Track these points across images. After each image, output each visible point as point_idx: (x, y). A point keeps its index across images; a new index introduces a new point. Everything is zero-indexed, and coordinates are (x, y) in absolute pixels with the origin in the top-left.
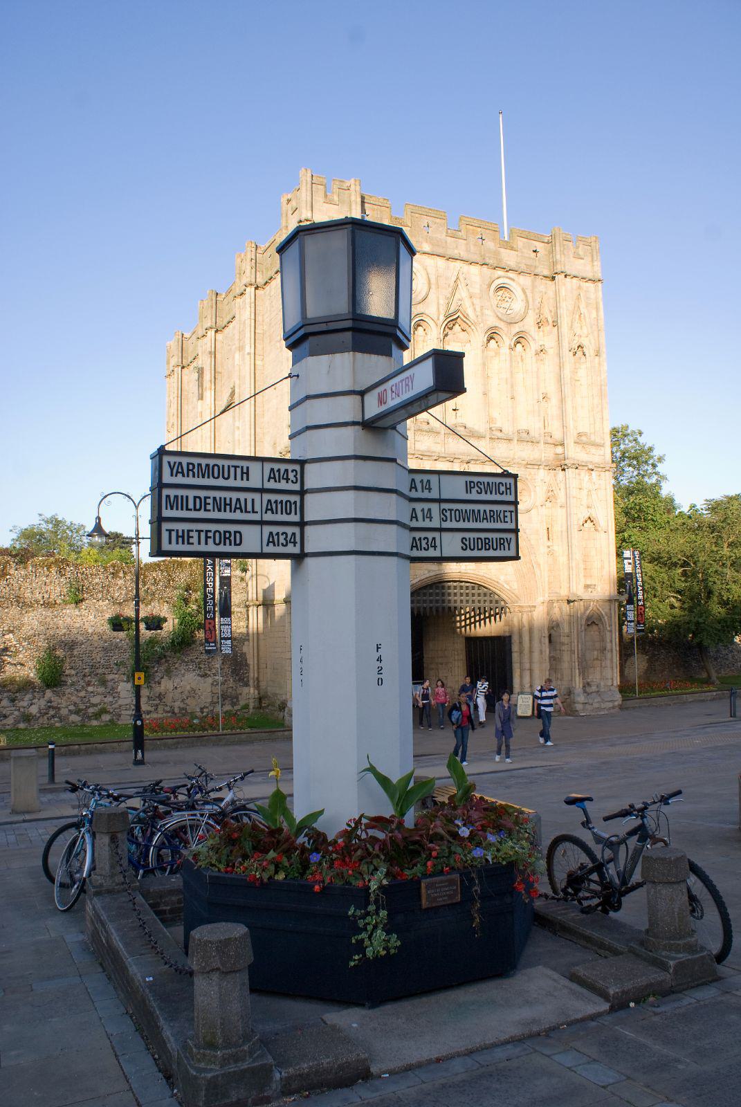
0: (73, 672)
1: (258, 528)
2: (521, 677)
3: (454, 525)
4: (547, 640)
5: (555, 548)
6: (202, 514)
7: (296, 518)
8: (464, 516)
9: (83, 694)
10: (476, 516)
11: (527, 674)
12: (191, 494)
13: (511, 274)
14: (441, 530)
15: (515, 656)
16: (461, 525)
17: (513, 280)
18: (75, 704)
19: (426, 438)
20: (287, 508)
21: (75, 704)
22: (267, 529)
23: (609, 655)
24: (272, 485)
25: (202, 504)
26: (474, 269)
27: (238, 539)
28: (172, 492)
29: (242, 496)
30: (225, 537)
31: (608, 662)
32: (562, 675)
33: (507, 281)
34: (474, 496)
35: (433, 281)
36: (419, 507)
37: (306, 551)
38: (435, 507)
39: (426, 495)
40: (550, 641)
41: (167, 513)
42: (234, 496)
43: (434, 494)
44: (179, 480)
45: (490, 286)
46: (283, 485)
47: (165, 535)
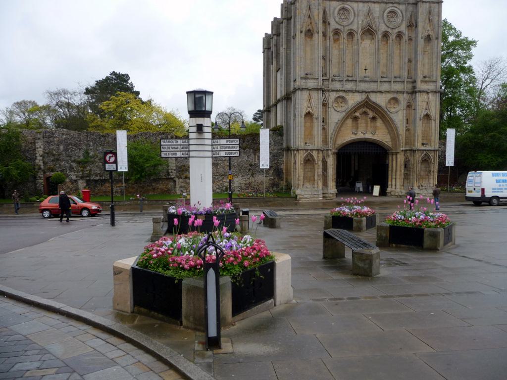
0: (218, 174)
1: (180, 152)
2: (392, 181)
3: (223, 150)
4: (403, 167)
5: (410, 128)
6: (169, 150)
7: (188, 150)
8: (226, 148)
9: (221, 182)
10: (229, 148)
11: (394, 180)
12: (167, 146)
13: (395, 5)
14: (220, 151)
15: (390, 172)
16: (225, 150)
17: (396, 7)
18: (219, 186)
19: (350, 83)
20: (186, 148)
21: (219, 186)
22: (182, 152)
23: (432, 174)
24: (182, 144)
25: (169, 148)
26: (377, 5)
27: (176, 154)
28: (163, 146)
29: (177, 146)
30: (174, 154)
31: (432, 177)
32: (410, 181)
33: (393, 8)
34: (229, 143)
35: (357, 13)
36: (215, 146)
37: (190, 156)
38: (219, 146)
39: (217, 144)
40: (405, 166)
41: (162, 150)
42: (175, 146)
43: (219, 144)
44: (165, 144)
45: (384, 12)
46: (185, 144)
47: (162, 154)
